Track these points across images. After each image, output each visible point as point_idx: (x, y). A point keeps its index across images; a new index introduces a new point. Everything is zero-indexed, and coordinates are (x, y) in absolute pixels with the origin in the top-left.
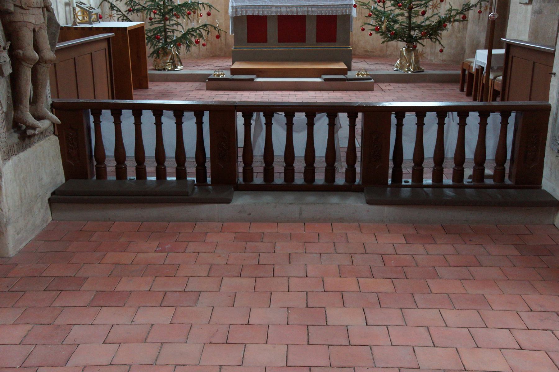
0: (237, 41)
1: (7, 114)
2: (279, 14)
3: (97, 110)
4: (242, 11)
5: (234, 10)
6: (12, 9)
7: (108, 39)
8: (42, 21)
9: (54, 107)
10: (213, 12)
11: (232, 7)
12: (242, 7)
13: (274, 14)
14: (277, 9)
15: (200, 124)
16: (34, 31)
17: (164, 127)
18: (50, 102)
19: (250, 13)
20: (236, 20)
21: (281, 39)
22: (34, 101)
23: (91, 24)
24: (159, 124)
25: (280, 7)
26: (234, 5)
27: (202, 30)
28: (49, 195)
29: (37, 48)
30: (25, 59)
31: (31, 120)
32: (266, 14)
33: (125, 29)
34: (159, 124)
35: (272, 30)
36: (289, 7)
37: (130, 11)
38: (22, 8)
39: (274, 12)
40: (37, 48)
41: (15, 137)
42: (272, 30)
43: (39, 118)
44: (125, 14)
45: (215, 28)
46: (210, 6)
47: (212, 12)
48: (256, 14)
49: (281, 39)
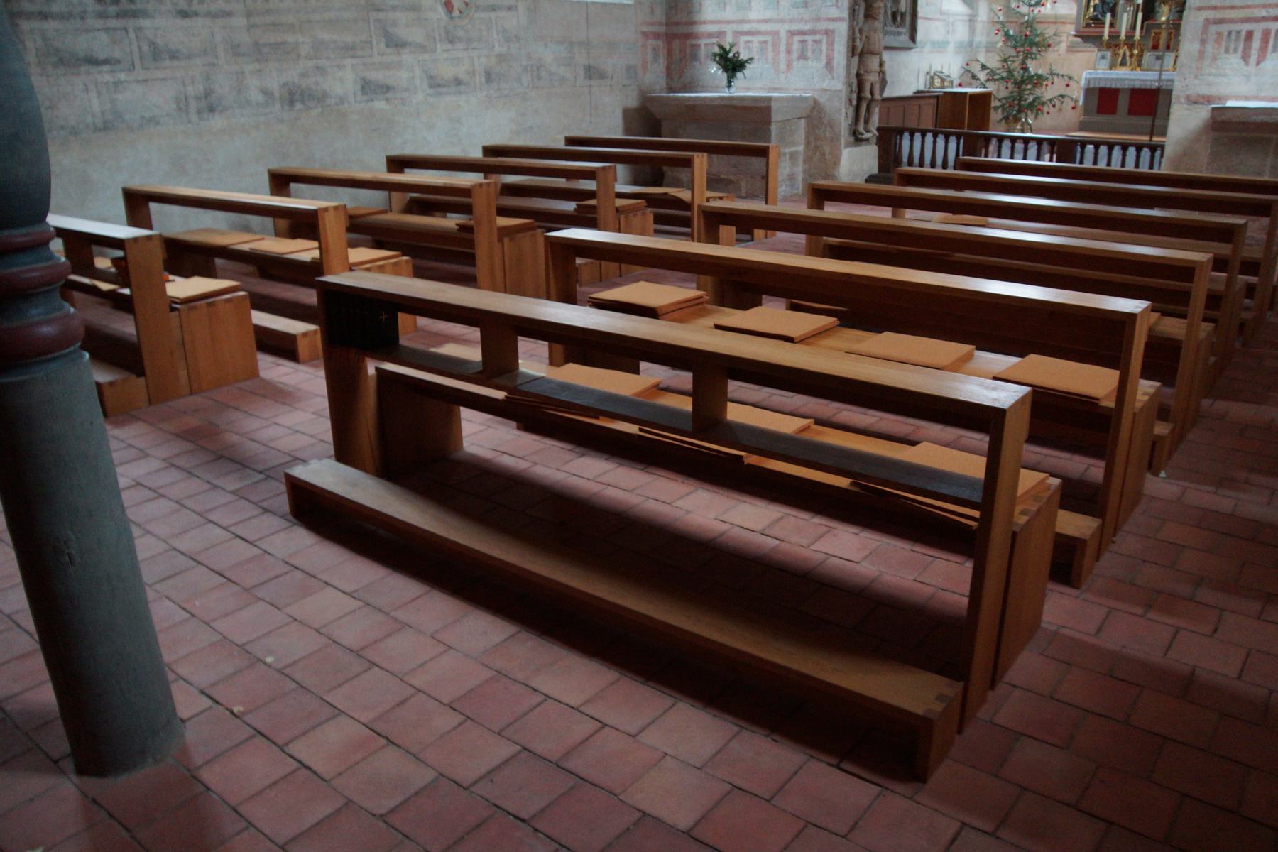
0: (1086, 111)
1: (850, 125)
2: (1131, 87)
3: (900, 132)
4: (1095, 83)
5: (1087, 82)
6: (862, 72)
7: (938, 97)
8: (877, 78)
9: (878, 129)
10: (1071, 83)
11: (1086, 79)
12: (1095, 79)
13: (1126, 87)
14: (1130, 83)
15: (958, 144)
16: (872, 84)
17: (937, 144)
18: (877, 125)
19: (1102, 85)
20: (1088, 92)
21: (1132, 111)
22: (866, 122)
23: (944, 88)
24: (935, 142)
25: (1134, 80)
26: (1088, 76)
27: (1055, 100)
28: (866, 177)
29: (872, 93)
30: (865, 98)
31: (861, 129)
32: (1118, 86)
33: (966, 93)
34: (935, 142)
35: (1123, 102)
36: (1143, 80)
37: (988, 80)
38: (867, 72)
39: (1126, 85)
40: (872, 93)
41: (852, 139)
42: (1123, 102)
43: (867, 131)
44: (984, 83)
45: (1072, 99)
46: (1070, 78)
47: (1070, 84)
48: (1108, 86)
49: (1132, 111)
